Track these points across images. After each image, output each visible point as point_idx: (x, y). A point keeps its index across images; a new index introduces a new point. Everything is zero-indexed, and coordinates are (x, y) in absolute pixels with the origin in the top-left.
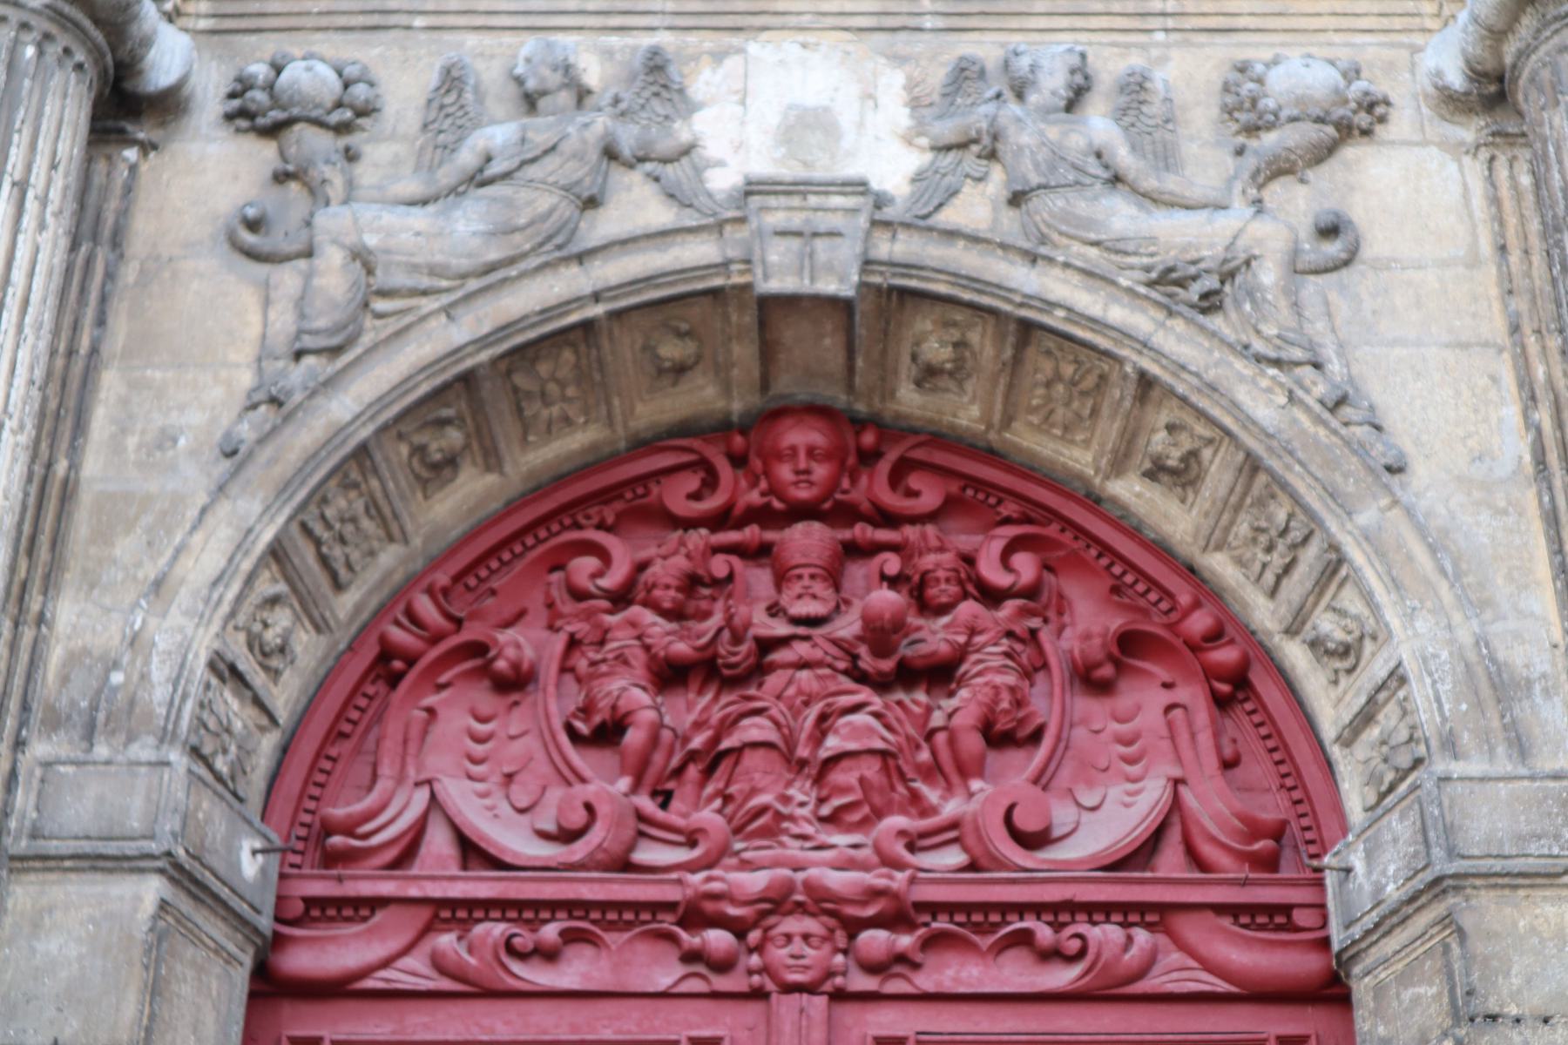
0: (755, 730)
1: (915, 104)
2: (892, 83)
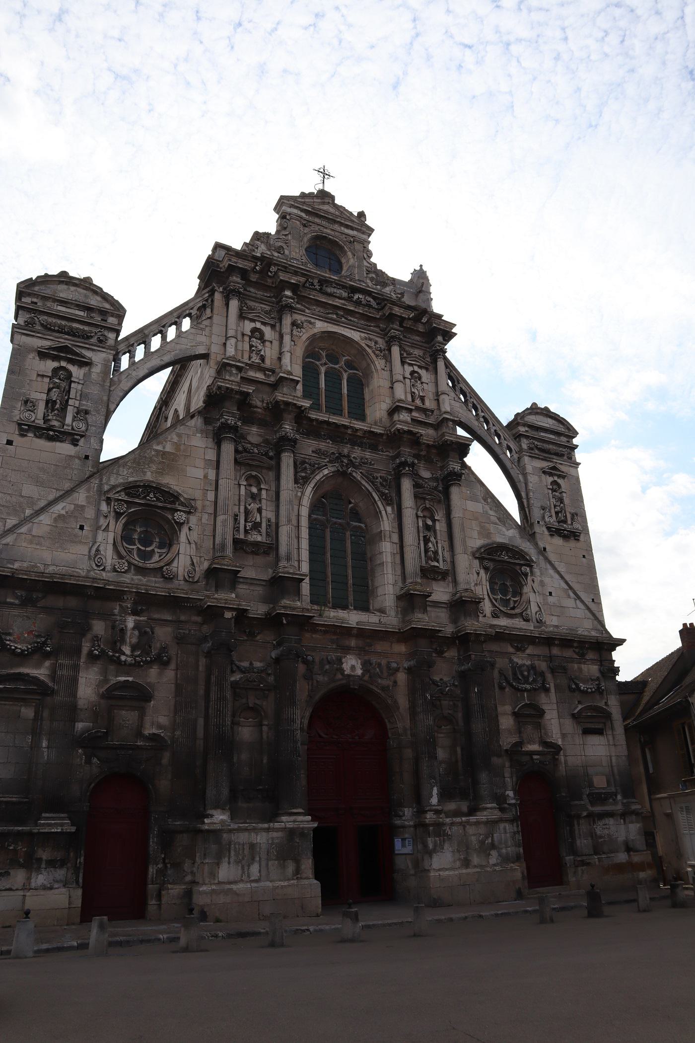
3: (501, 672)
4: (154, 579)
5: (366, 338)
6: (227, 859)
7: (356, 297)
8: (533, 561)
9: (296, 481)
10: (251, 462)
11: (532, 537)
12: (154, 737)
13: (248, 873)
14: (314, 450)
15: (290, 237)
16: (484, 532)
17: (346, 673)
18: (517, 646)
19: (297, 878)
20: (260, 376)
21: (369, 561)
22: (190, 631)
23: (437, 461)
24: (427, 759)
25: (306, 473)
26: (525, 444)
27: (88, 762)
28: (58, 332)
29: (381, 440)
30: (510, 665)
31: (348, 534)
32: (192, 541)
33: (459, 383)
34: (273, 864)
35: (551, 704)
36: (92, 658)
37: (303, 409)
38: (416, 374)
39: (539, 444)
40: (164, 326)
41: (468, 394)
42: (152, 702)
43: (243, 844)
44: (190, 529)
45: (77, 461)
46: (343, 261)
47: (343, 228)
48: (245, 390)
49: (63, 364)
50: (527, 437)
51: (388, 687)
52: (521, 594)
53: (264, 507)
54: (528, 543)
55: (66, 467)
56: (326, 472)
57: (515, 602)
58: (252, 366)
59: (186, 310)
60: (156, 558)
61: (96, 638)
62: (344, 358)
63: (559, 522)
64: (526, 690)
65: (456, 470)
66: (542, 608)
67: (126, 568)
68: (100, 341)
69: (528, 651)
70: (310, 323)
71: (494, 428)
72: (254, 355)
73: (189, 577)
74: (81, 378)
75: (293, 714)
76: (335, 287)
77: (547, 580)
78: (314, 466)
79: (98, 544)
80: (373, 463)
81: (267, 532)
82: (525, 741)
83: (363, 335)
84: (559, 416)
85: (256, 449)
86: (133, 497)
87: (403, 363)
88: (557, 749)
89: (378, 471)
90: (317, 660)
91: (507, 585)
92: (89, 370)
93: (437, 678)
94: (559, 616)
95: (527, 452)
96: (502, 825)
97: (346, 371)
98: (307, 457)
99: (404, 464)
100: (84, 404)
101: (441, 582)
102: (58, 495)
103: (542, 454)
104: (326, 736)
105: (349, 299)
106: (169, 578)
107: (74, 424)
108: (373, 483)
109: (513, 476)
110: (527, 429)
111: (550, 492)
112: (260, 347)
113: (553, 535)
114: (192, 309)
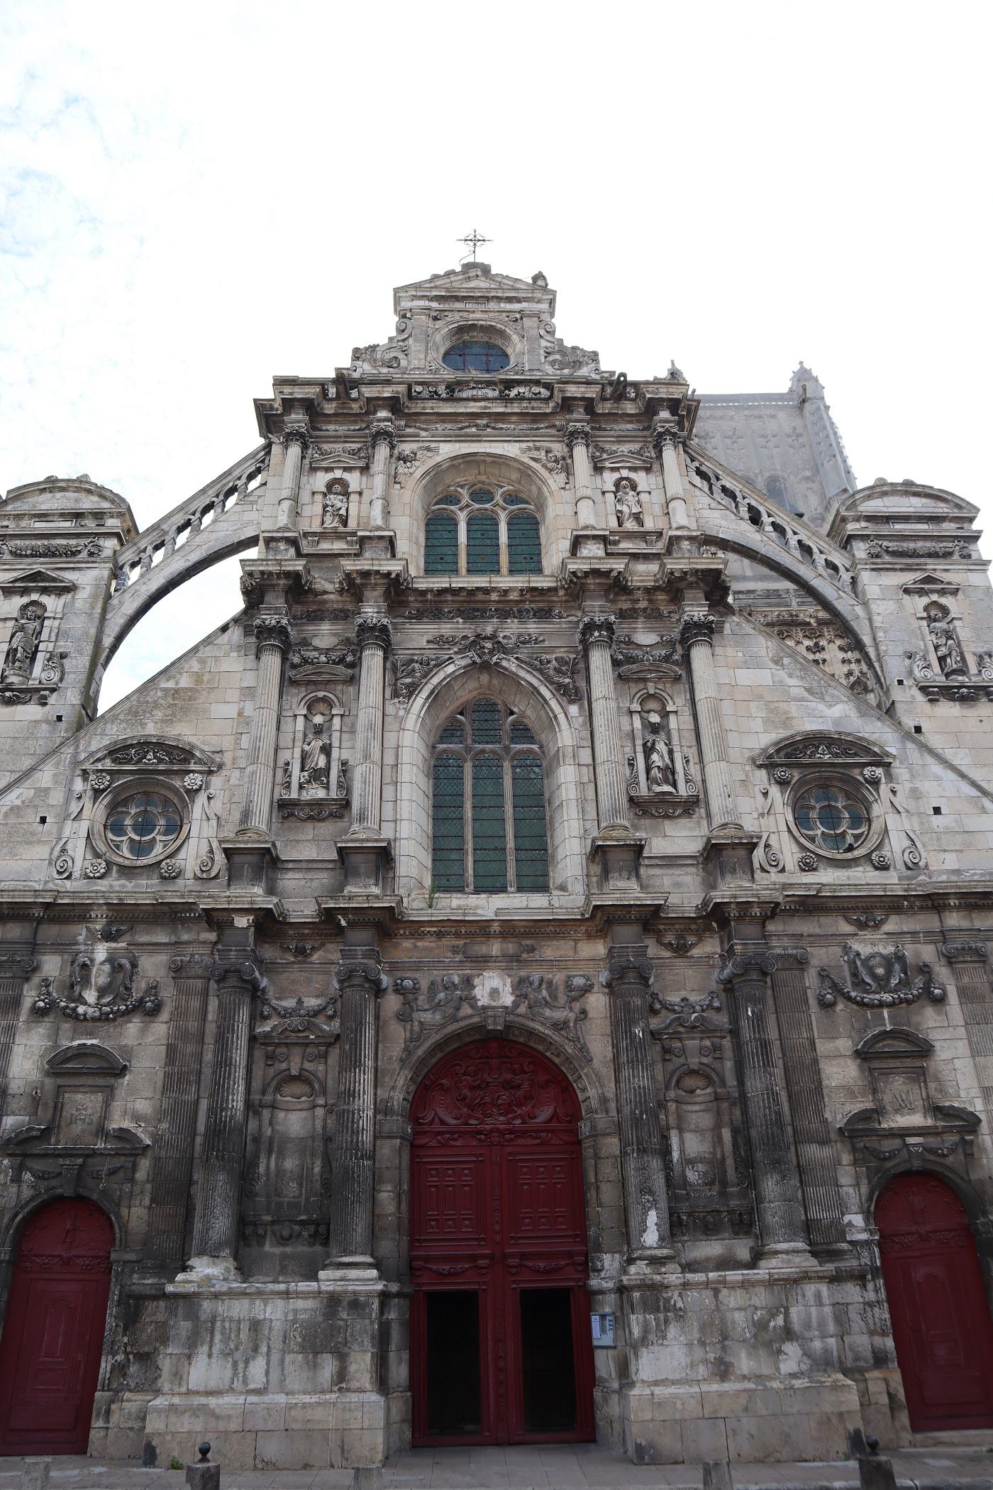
0: (487, 1099)
1: (512, 986)
2: (509, 980)
3: (824, 973)
4: (145, 882)
5: (529, 449)
6: (206, 1348)
7: (513, 393)
8: (888, 754)
9: (396, 694)
10: (313, 678)
11: (889, 711)
13: (244, 1375)
14: (431, 638)
15: (411, 341)
16: (775, 716)
17: (480, 1004)
18: (858, 920)
19: (340, 1389)
20: (339, 546)
21: (547, 805)
22: (192, 955)
23: (670, 612)
24: (635, 1155)
25: (414, 677)
26: (860, 550)
27: (17, 1179)
28: (32, 556)
29: (555, 599)
30: (846, 958)
31: (507, 765)
32: (212, 816)
33: (718, 479)
34: (295, 1360)
35: (951, 1029)
36: (38, 1013)
37: (393, 576)
38: (624, 482)
39: (890, 544)
40: (194, 514)
41: (738, 494)
42: (127, 1078)
43: (239, 1321)
44: (209, 798)
45: (44, 726)
46: (509, 351)
47: (502, 305)
48: (290, 568)
49: (34, 597)
50: (864, 538)
51: (566, 1022)
52: (869, 821)
53: (336, 743)
54: (879, 724)
55: (28, 738)
56: (450, 669)
57: (857, 837)
58: (323, 536)
59: (229, 482)
60: (158, 848)
61: (46, 983)
62: (501, 491)
63: (947, 675)
64: (882, 1005)
65: (696, 619)
66: (916, 840)
67: (103, 871)
68: (91, 554)
69: (889, 927)
70: (428, 449)
71: (796, 538)
72: (328, 519)
73: (203, 871)
74: (59, 609)
75: (355, 1082)
76: (473, 388)
77: (926, 786)
78: (428, 664)
79: (65, 840)
80: (541, 638)
81: (339, 782)
82: (889, 1108)
83: (524, 445)
84: (931, 488)
85: (323, 656)
86: (120, 763)
87: (598, 469)
88: (970, 1123)
89: (552, 649)
90: (424, 984)
91: (836, 808)
92: (73, 597)
93: (674, 998)
94: (961, 851)
95: (866, 564)
96: (810, 1289)
97: (505, 509)
98: (418, 652)
99: (590, 627)
100: (61, 646)
101: (684, 822)
102: (12, 779)
103: (896, 560)
104: (455, 1122)
105: (504, 398)
106: (171, 877)
107: (43, 676)
108: (541, 671)
109: (842, 612)
110: (863, 524)
111: (924, 623)
112: (339, 505)
113: (937, 700)
114: (239, 478)
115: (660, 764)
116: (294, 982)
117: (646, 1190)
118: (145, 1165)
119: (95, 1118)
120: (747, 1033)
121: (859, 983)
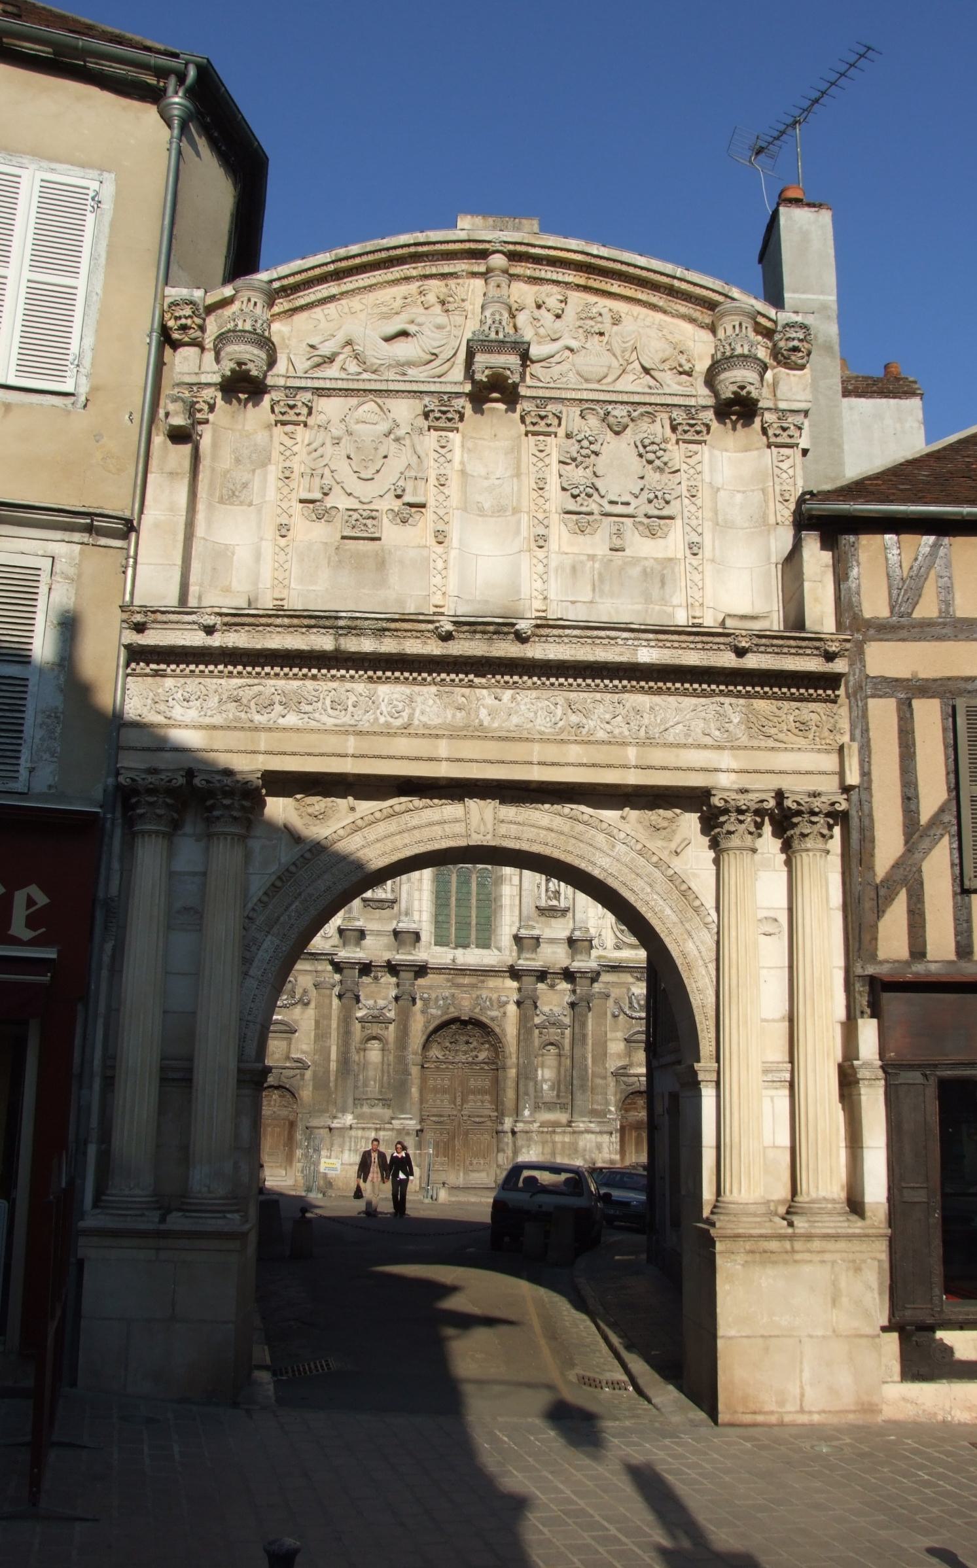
12: (298, 1061)
31: (474, 876)
93: (546, 1009)
96: (589, 1136)
101: (561, 920)
115: (553, 889)
116: (372, 992)
117: (527, 1094)
118: (308, 1074)
119: (285, 1052)
120: (577, 1030)
121: (631, 1007)
